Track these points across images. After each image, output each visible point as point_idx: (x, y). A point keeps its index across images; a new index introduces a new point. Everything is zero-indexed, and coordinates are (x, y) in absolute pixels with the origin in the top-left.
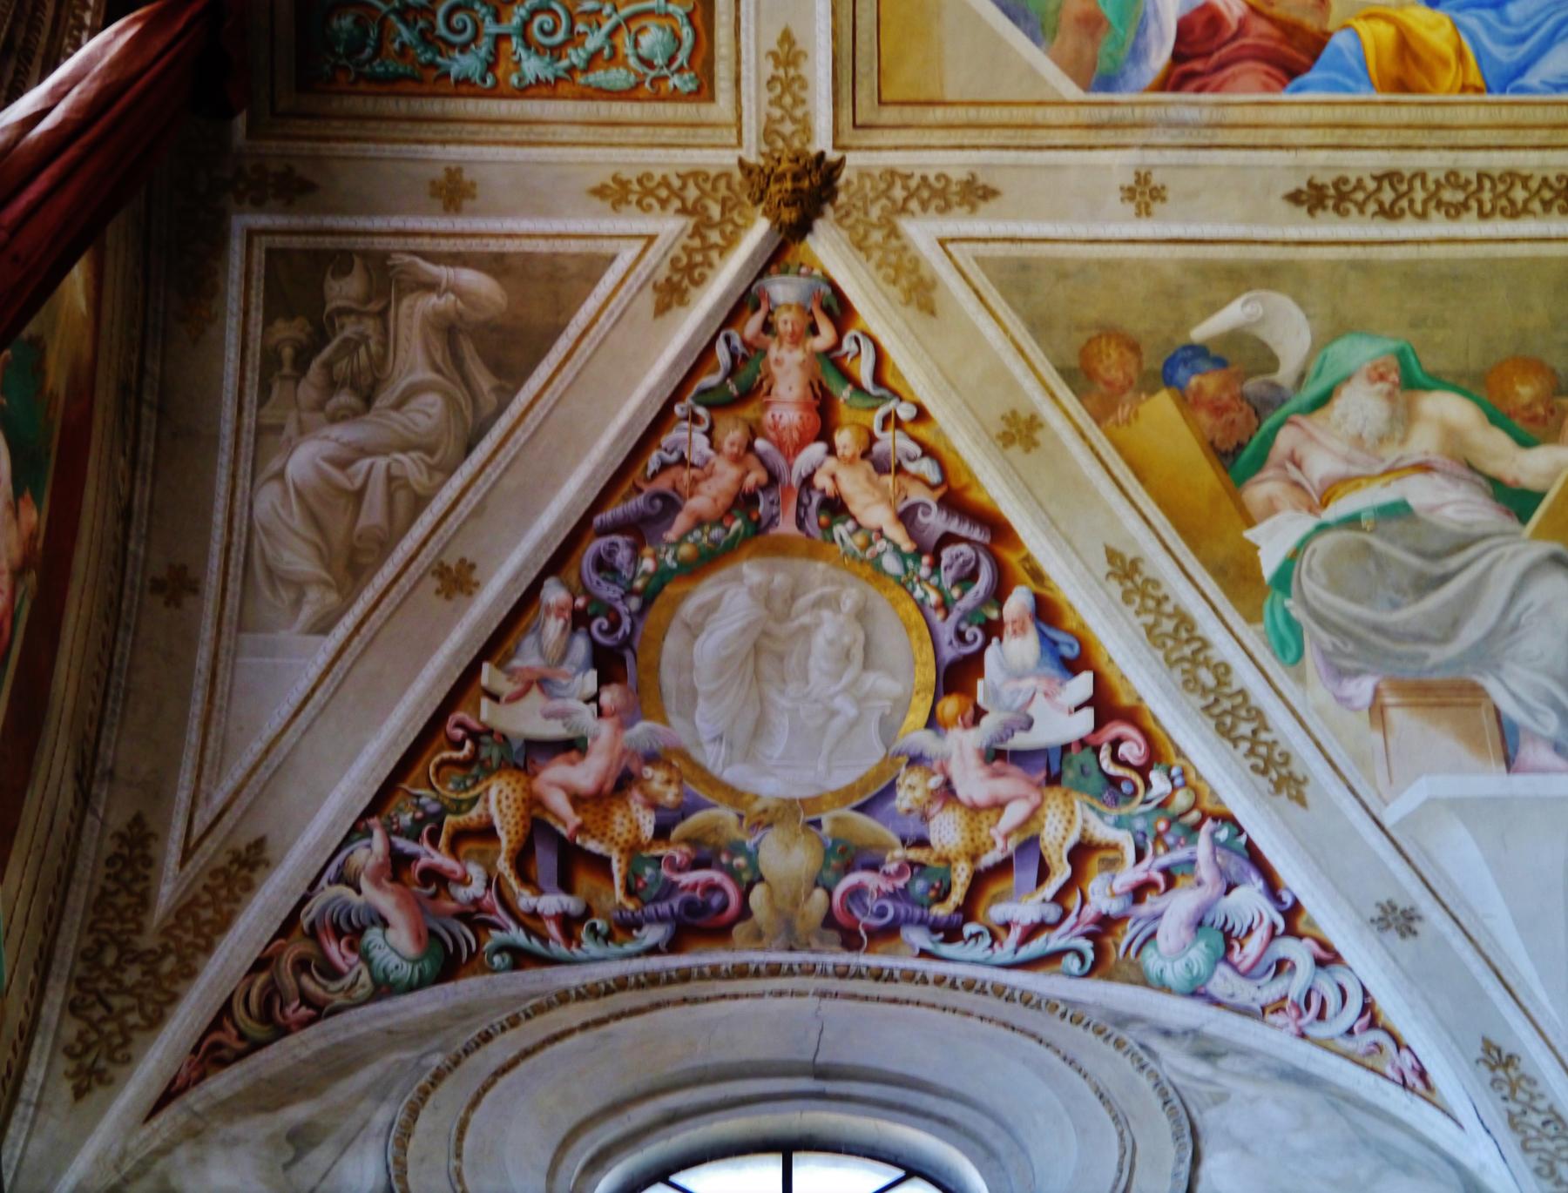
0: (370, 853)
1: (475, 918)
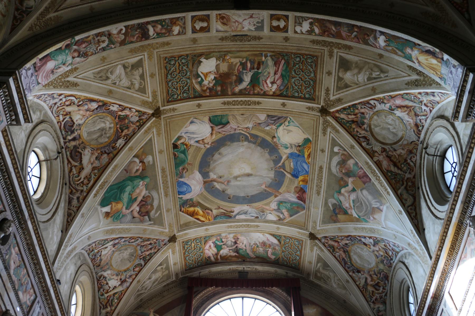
0: (372, 305)
1: (381, 297)
